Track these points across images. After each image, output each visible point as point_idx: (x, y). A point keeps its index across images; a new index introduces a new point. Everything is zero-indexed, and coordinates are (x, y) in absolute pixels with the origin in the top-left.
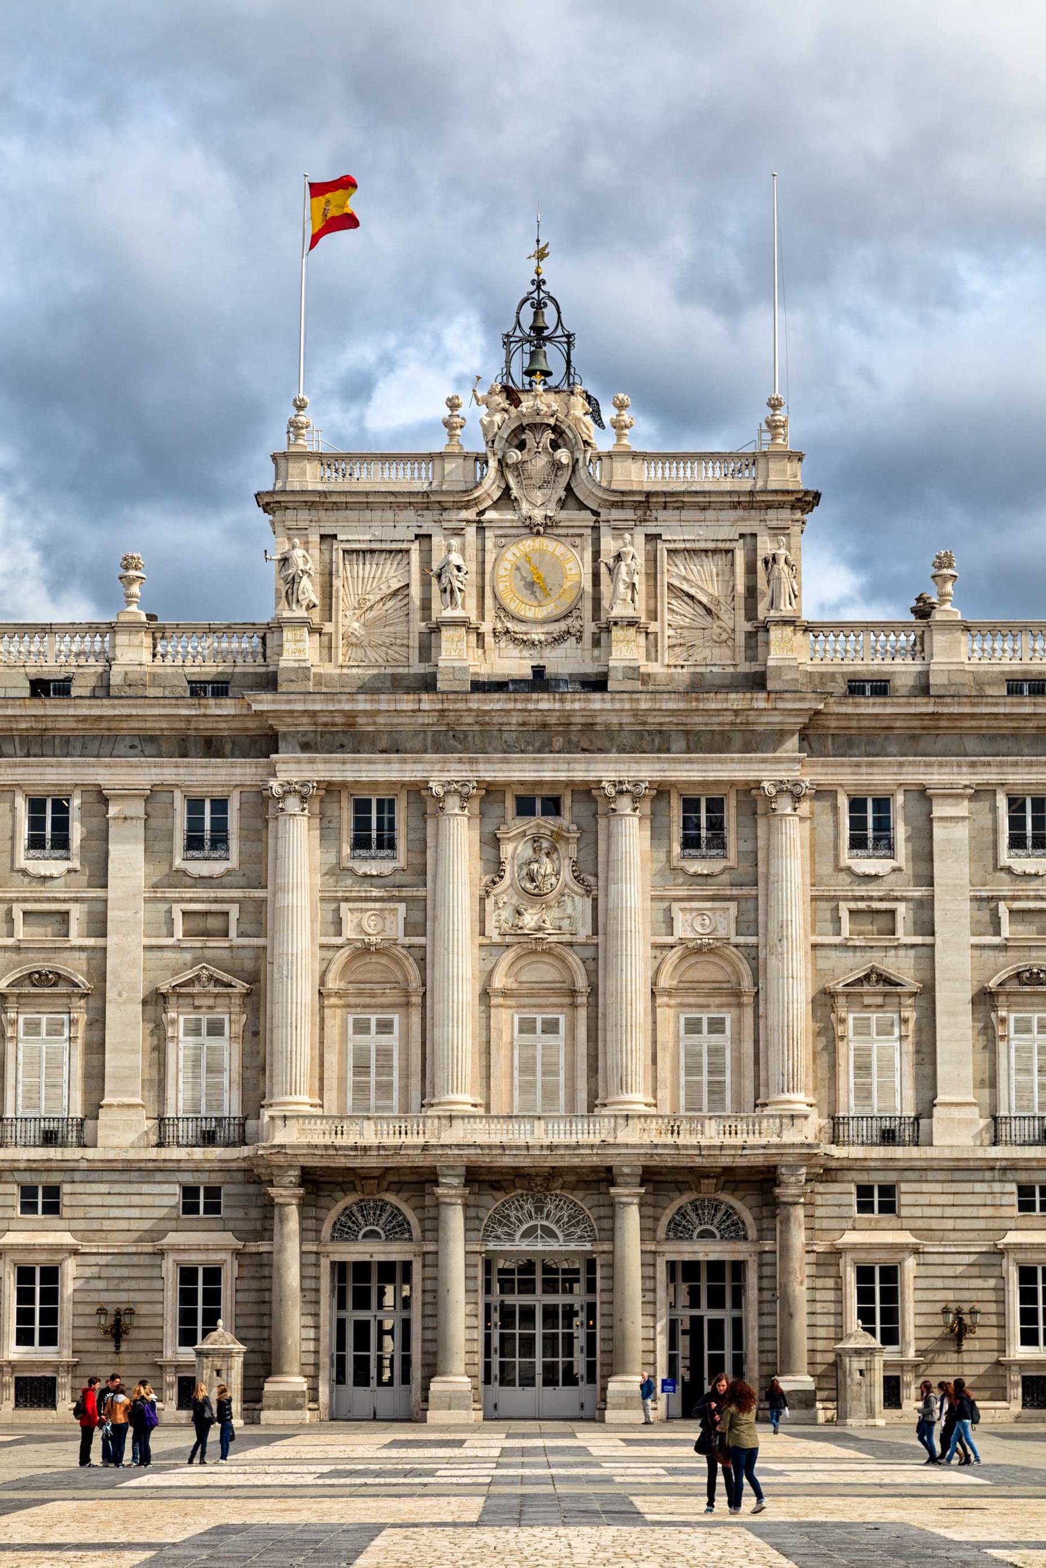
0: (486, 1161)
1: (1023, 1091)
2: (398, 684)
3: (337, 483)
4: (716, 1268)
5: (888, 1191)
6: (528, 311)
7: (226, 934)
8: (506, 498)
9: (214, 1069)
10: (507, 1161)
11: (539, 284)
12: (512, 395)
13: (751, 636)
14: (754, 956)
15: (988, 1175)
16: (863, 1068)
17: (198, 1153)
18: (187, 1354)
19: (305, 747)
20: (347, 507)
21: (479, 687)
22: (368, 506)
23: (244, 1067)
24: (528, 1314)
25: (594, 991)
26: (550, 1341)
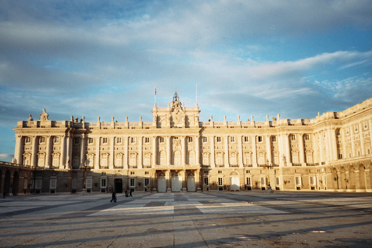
1: (219, 162)
5: (207, 171)
9: (148, 161)
11: (176, 93)
12: (174, 102)
15: (216, 170)
16: (205, 161)
18: (146, 186)
19: (156, 133)
20: (159, 112)
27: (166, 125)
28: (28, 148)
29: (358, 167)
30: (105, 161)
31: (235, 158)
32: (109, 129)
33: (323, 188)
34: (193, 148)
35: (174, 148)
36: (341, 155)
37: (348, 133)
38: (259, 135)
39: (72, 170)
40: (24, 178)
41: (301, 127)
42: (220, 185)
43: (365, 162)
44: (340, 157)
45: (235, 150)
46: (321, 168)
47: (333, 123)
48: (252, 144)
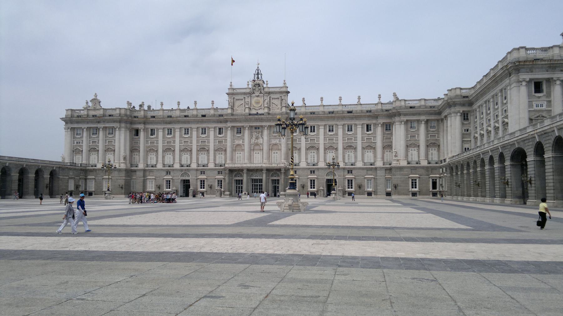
1: (311, 160)
3: (235, 91)
4: (275, 180)
6: (257, 71)
8: (254, 93)
11: (258, 68)
12: (254, 81)
13: (281, 108)
14: (280, 144)
17: (219, 168)
19: (231, 122)
20: (236, 94)
21: (250, 114)
22: (238, 94)
24: (257, 185)
25: (263, 149)
26: (260, 188)
27: (245, 111)
30: (170, 158)
32: (173, 118)
35: (253, 141)
40: (68, 177)
41: (424, 111)
45: (334, 143)
48: (357, 135)
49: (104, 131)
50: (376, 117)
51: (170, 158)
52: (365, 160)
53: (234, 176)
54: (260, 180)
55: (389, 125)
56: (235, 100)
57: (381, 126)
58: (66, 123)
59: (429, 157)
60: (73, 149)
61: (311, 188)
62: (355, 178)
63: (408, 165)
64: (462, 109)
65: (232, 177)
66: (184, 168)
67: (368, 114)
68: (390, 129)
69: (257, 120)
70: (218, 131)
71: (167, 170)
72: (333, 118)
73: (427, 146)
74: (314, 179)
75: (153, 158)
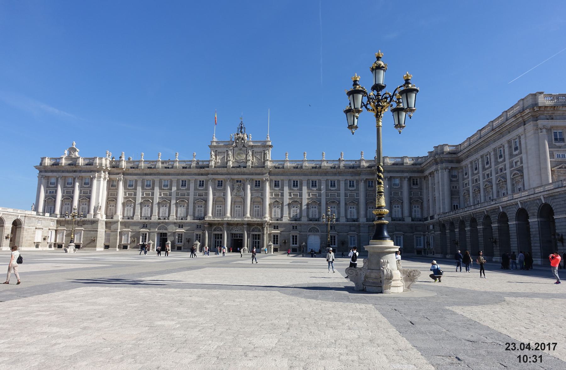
0: (229, 222)
2: (224, 167)
7: (203, 196)
10: (231, 222)
16: (275, 212)
20: (219, 147)
23: (204, 211)
28: (52, 191)
29: (469, 223)
31: (315, 209)
33: (431, 253)
34: (260, 195)
36: (457, 206)
37: (466, 174)
38: (349, 178)
39: (106, 220)
42: (293, 246)
43: (477, 214)
44: (454, 208)
46: (429, 224)
47: (445, 160)
49: (80, 181)
50: (359, 174)
51: (148, 210)
52: (348, 216)
53: (213, 230)
54: (240, 234)
55: (372, 182)
56: (217, 153)
57: (364, 182)
58: (40, 172)
59: (412, 214)
60: (45, 198)
61: (293, 244)
62: (338, 234)
63: (392, 222)
64: (450, 165)
65: (211, 231)
66: (161, 220)
67: (351, 170)
68: (372, 186)
69: (239, 174)
70: (198, 183)
71: (145, 223)
72: (317, 174)
73: (410, 203)
74: (296, 234)
75: (130, 210)
